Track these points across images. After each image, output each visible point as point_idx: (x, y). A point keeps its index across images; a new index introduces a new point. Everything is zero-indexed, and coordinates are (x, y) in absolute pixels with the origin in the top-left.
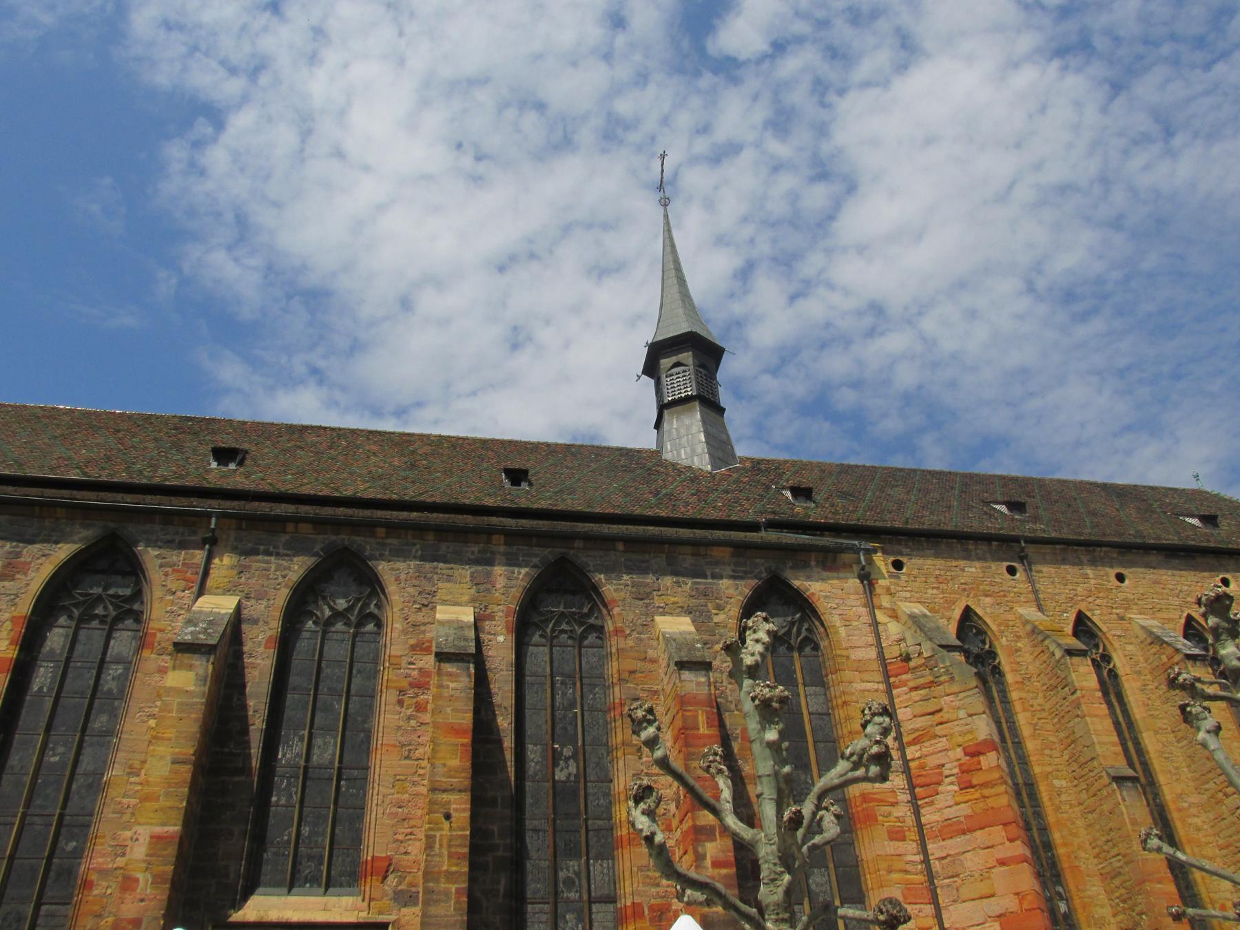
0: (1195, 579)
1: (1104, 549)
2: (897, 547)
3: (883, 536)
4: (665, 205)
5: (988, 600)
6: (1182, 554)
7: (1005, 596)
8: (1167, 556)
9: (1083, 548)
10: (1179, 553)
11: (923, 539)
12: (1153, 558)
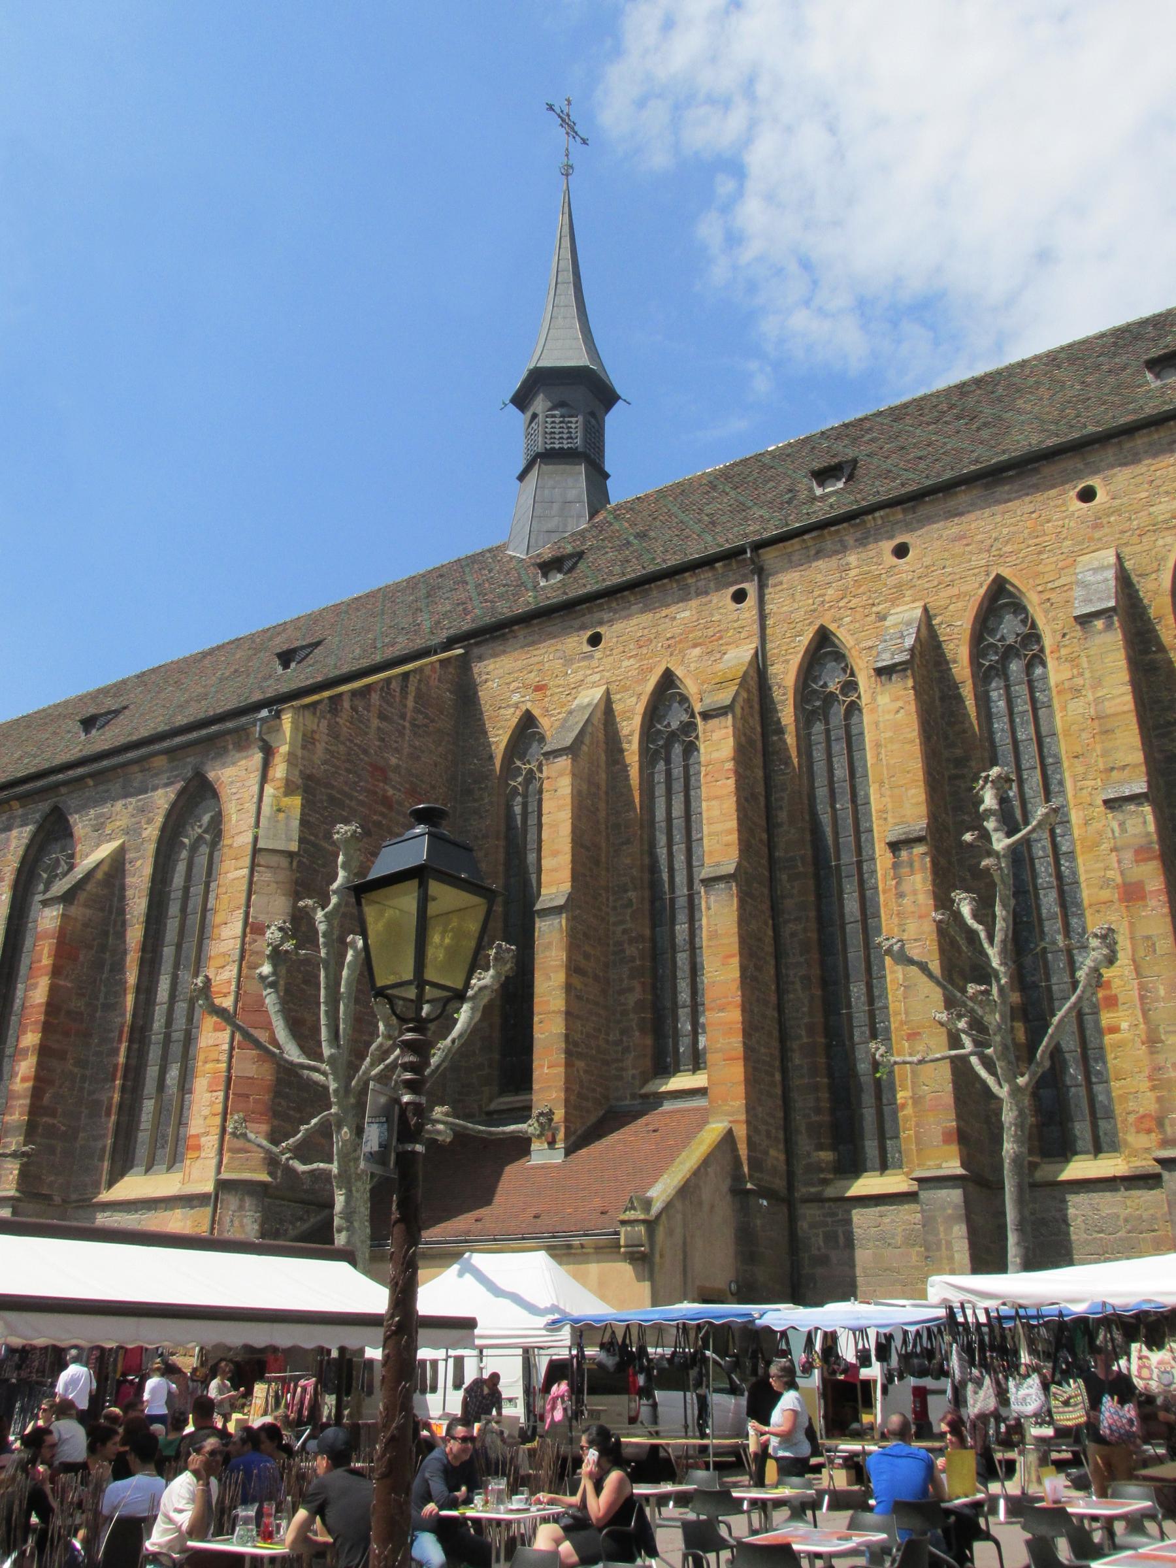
0: (1031, 508)
1: (877, 514)
2: (587, 619)
3: (578, 608)
4: (567, 175)
5: (697, 651)
6: (1011, 473)
7: (721, 638)
8: (987, 486)
9: (845, 525)
10: (1004, 475)
11: (626, 593)
12: (963, 497)
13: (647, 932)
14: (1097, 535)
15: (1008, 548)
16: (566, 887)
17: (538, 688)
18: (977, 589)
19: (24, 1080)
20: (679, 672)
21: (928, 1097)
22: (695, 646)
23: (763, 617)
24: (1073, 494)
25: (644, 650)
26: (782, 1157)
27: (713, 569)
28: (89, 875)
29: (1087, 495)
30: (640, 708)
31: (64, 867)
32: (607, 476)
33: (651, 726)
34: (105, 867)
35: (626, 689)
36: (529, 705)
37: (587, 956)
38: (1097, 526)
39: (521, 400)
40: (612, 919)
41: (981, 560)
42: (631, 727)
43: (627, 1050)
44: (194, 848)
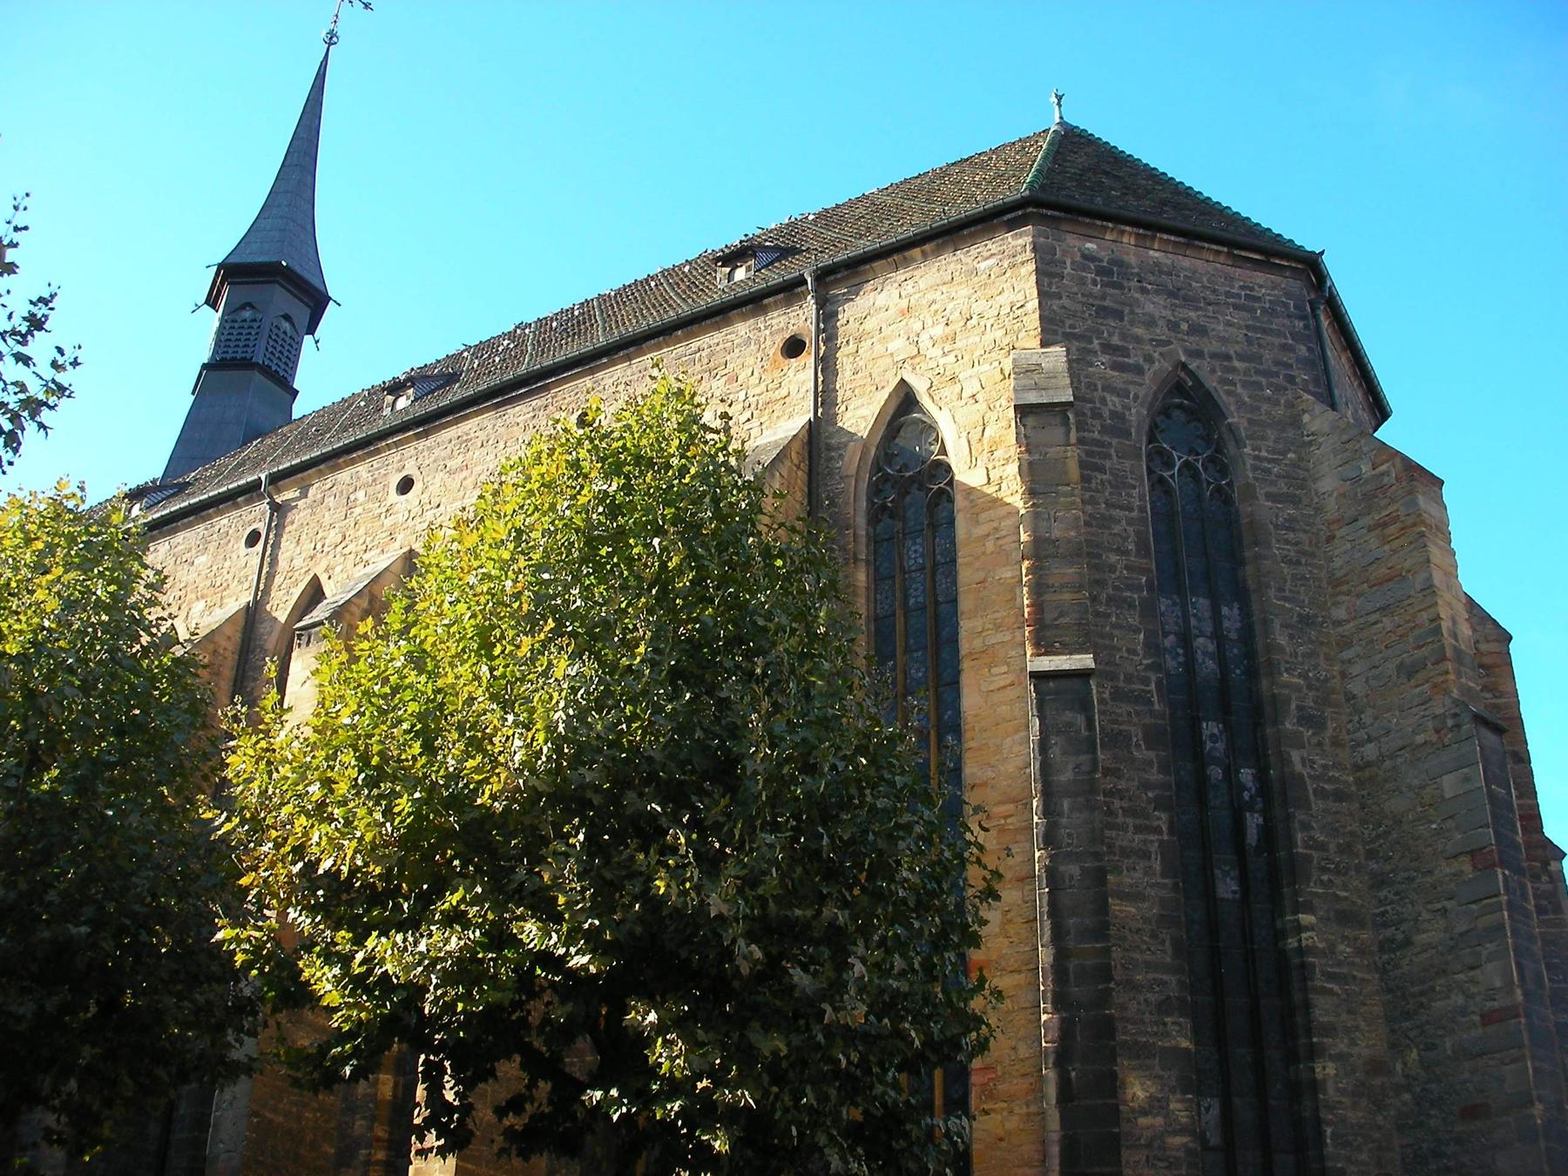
21: (223, 1157)
32: (296, 392)
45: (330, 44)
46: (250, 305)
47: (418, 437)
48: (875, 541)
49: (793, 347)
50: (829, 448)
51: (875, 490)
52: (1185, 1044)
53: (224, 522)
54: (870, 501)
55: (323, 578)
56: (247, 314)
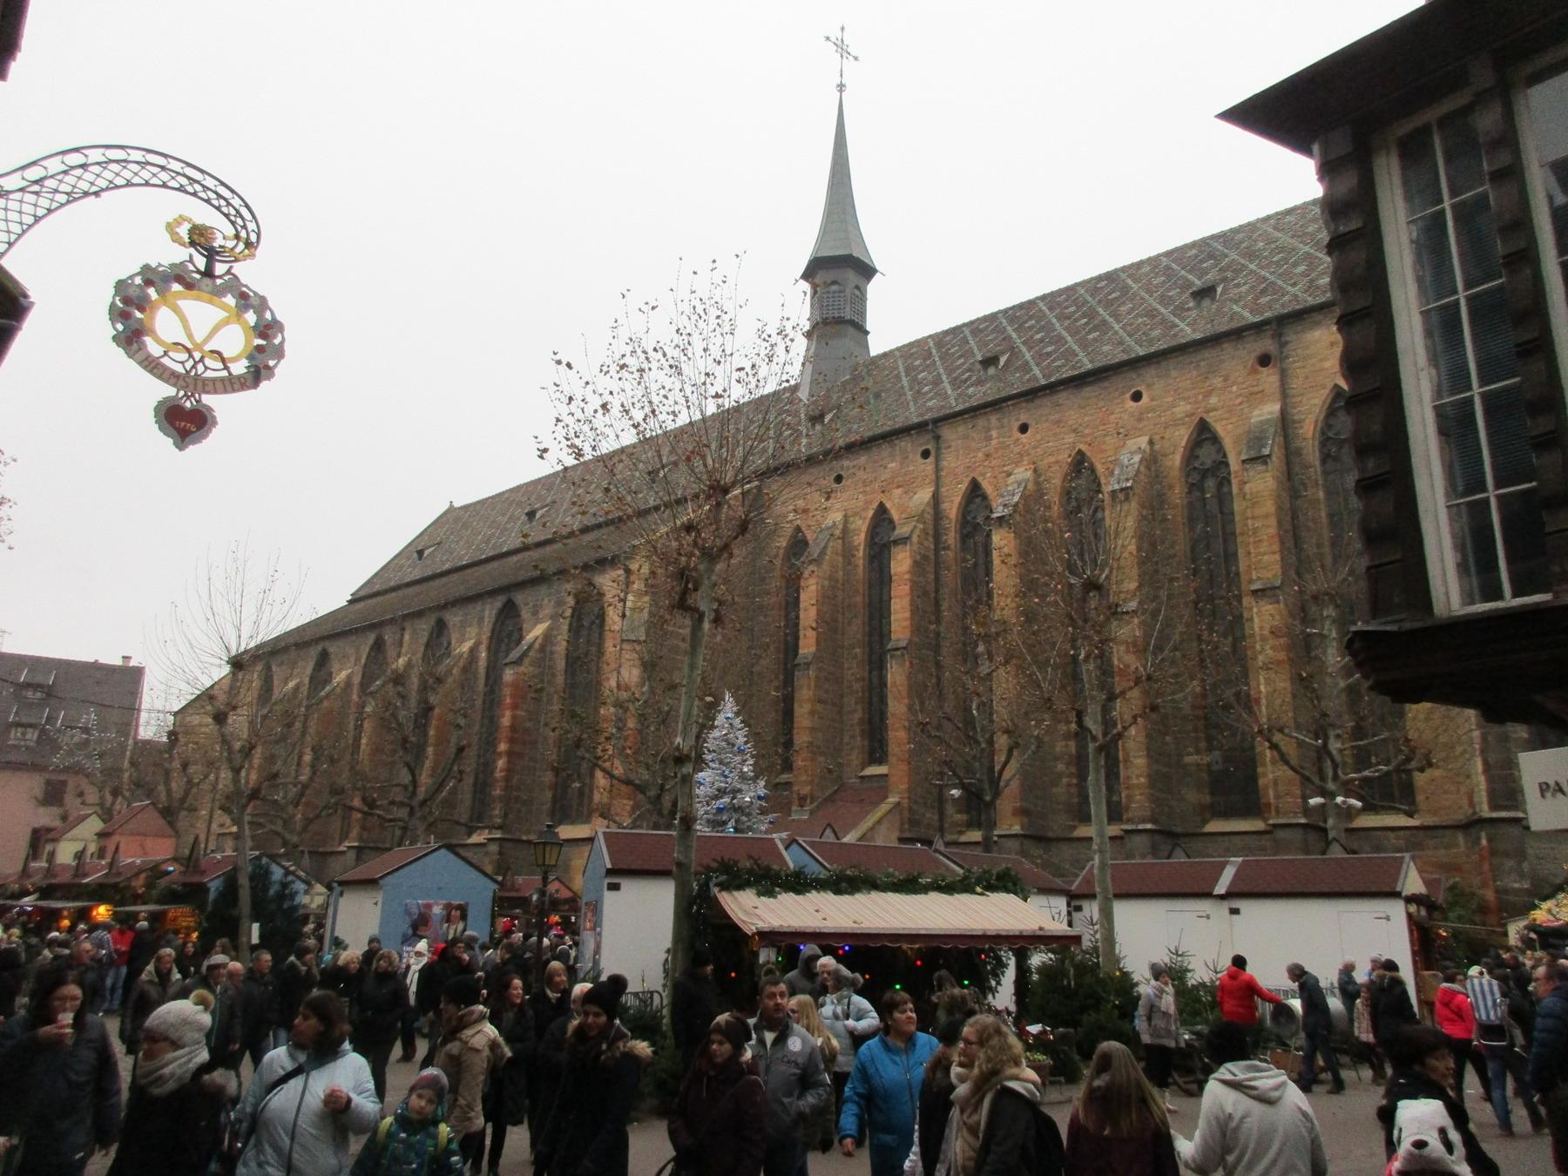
5: (899, 491)
8: (1077, 386)
13: (866, 674)
14: (1141, 425)
15: (1087, 431)
16: (813, 649)
17: (805, 511)
18: (1065, 457)
19: (501, 771)
20: (888, 505)
22: (898, 487)
23: (938, 469)
24: (1128, 395)
25: (868, 489)
26: (936, 817)
27: (910, 435)
28: (530, 647)
29: (1137, 397)
30: (864, 528)
31: (516, 636)
33: (872, 538)
34: (539, 641)
35: (855, 514)
36: (798, 522)
37: (827, 691)
38: (1140, 420)
39: (808, 275)
40: (846, 666)
41: (1070, 438)
42: (860, 539)
43: (853, 748)
44: (590, 629)
45: (841, 91)
46: (834, 283)
47: (1027, 401)
48: (1325, 473)
49: (1264, 360)
50: (1294, 422)
51: (1323, 444)
52: (1526, 736)
53: (904, 444)
54: (1321, 452)
55: (980, 479)
56: (834, 288)
